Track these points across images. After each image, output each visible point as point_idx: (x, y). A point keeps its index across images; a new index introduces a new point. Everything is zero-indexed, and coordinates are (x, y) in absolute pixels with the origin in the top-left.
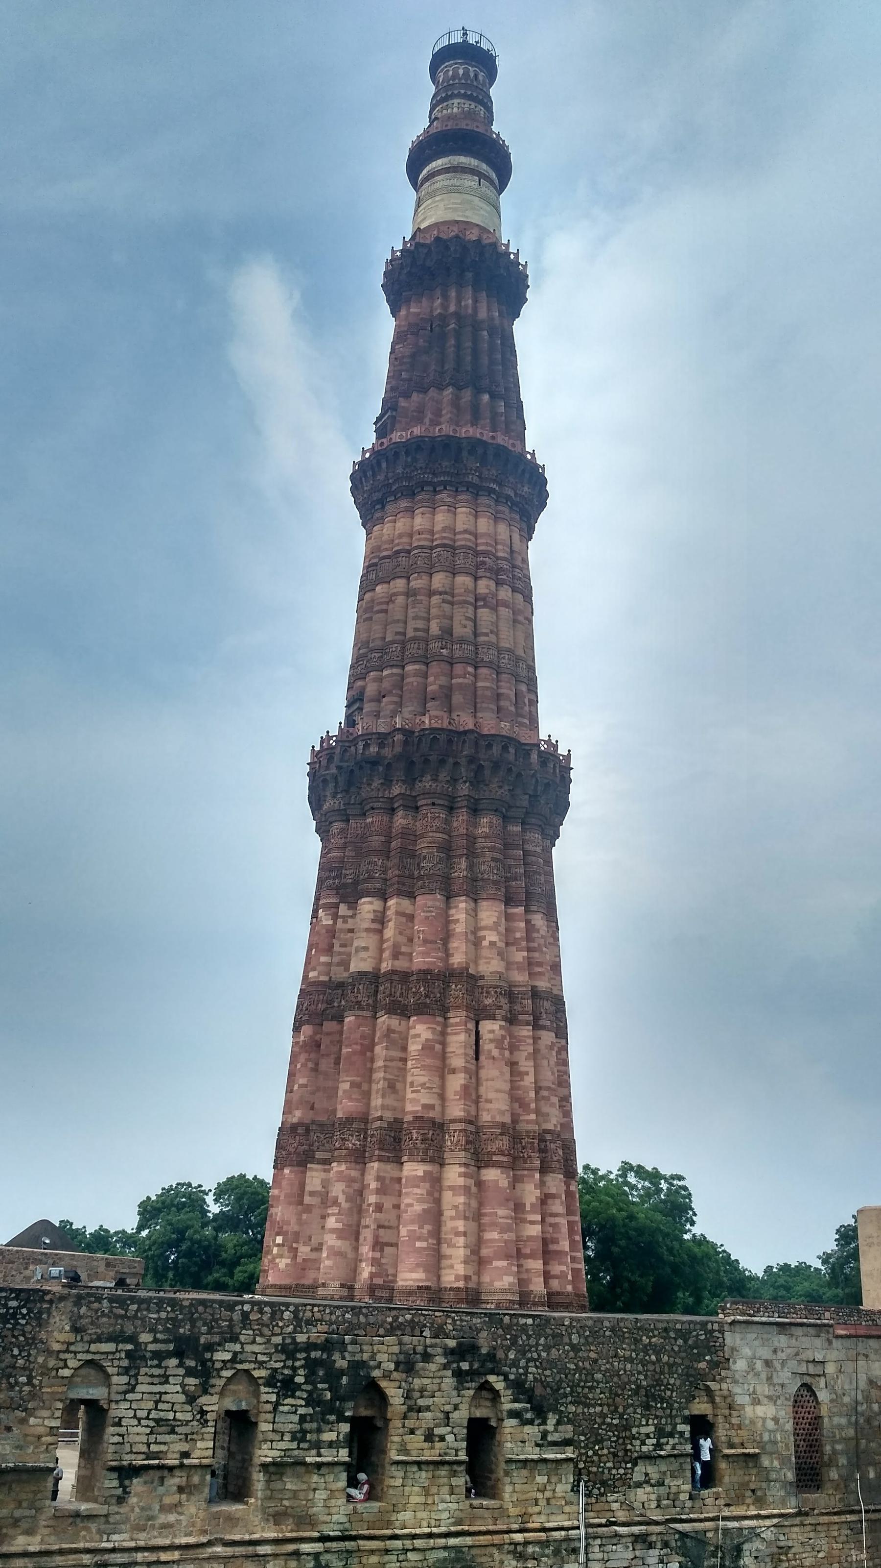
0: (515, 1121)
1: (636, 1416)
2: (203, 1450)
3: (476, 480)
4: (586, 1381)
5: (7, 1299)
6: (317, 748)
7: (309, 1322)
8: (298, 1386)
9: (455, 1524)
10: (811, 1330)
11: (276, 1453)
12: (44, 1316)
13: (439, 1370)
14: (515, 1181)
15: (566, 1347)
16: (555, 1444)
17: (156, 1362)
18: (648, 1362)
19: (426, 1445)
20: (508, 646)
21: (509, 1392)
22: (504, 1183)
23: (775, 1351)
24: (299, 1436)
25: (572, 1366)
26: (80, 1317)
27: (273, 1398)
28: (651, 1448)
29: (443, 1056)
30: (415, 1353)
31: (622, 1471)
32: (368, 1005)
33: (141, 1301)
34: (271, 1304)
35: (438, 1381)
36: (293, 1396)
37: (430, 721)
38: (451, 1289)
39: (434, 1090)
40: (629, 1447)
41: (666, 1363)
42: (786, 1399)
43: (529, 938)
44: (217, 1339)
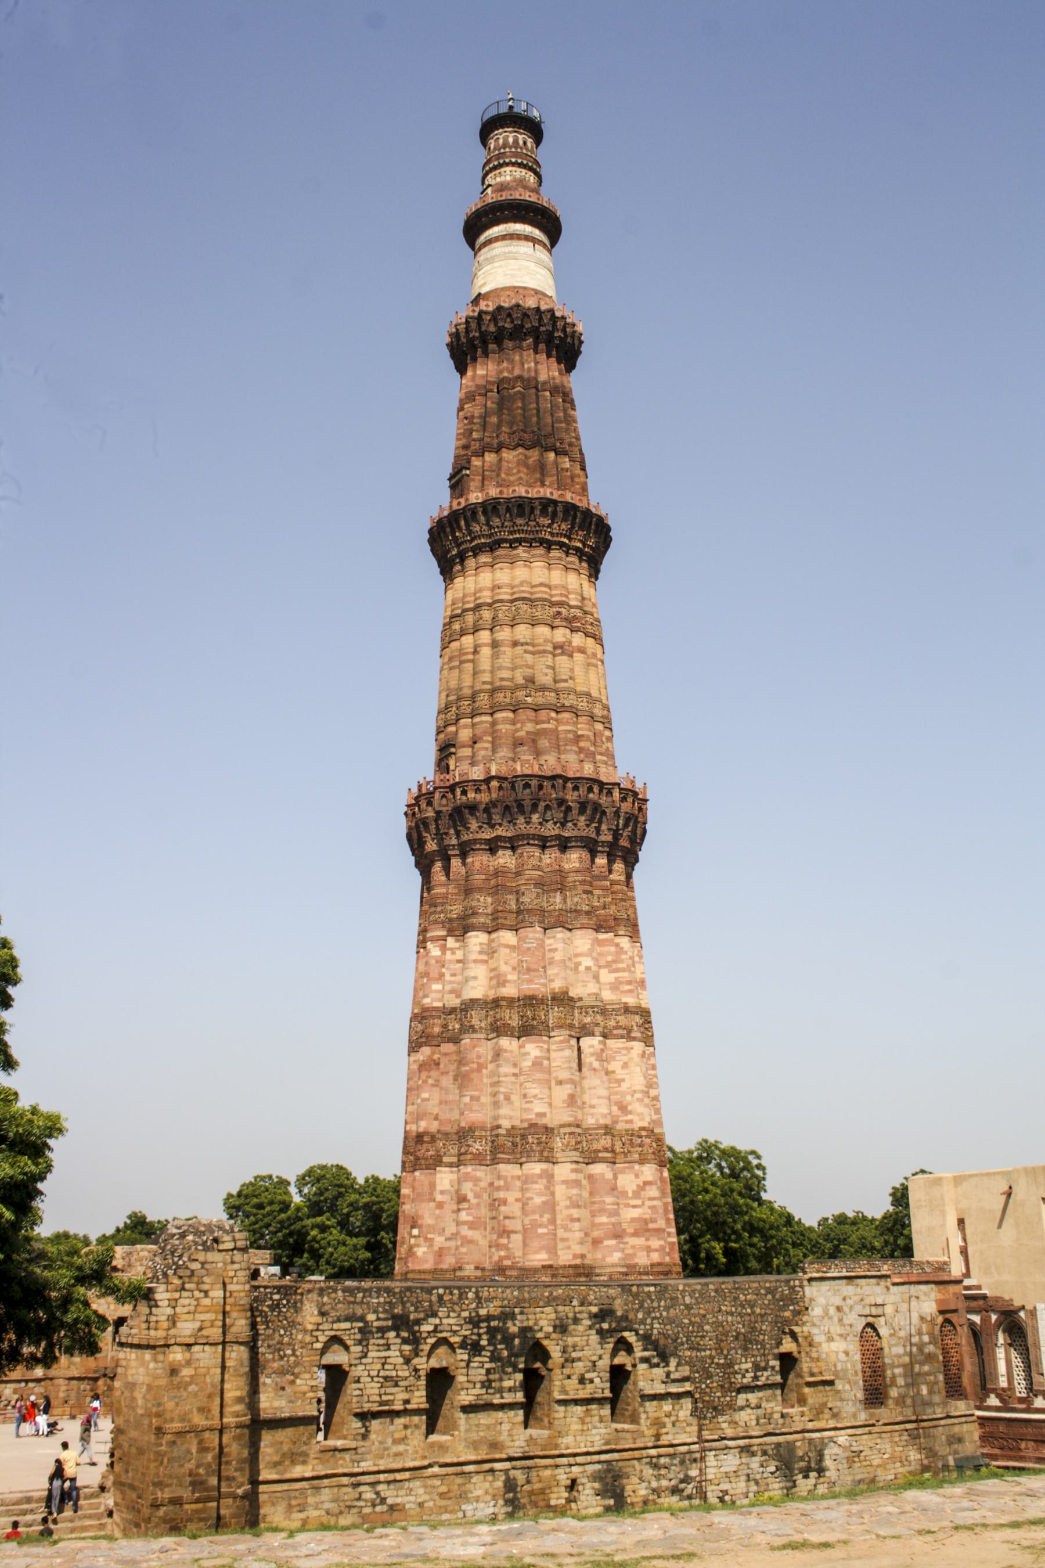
2: (419, 1398)
5: (272, 1293)
6: (415, 791)
8: (483, 1348)
10: (873, 1281)
11: (471, 1398)
12: (299, 1305)
16: (674, 1381)
17: (380, 1335)
19: (581, 1386)
21: (640, 1343)
22: (609, 1175)
23: (844, 1299)
24: (487, 1384)
25: (686, 1321)
26: (324, 1304)
27: (466, 1357)
30: (567, 1318)
31: (728, 1399)
33: (365, 1291)
34: (459, 1288)
36: (480, 1355)
37: (522, 766)
38: (570, 1266)
40: (733, 1380)
44: (422, 1315)
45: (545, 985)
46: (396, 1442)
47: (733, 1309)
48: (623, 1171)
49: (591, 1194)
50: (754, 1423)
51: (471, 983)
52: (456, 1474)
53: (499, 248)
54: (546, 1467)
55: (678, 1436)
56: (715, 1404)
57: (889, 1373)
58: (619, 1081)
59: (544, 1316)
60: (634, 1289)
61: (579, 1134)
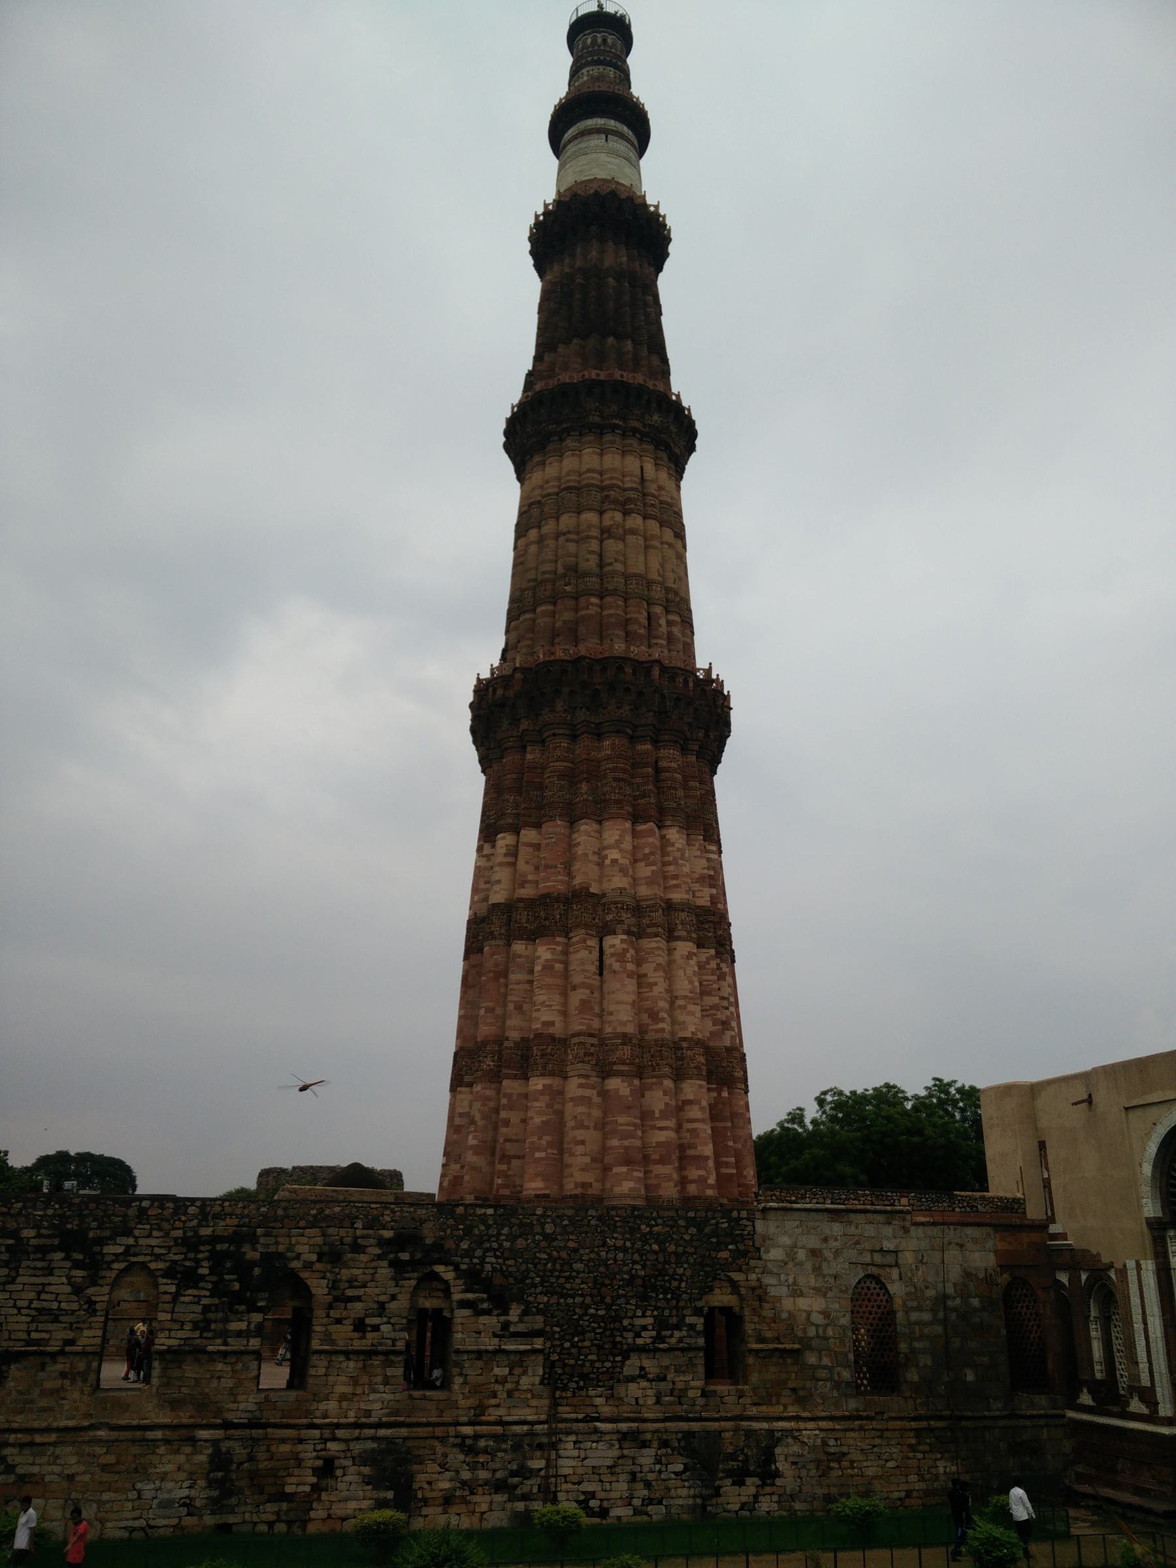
0: (642, 1029)
1: (628, 1307)
3: (597, 419)
4: (561, 1271)
7: (216, 1216)
8: (202, 1278)
9: (387, 1415)
10: (880, 1218)
14: (641, 1093)
15: (537, 1237)
17: (39, 1256)
18: (648, 1252)
19: (356, 1335)
21: (461, 1282)
23: (825, 1240)
27: (173, 1289)
29: (566, 975)
30: (342, 1244)
35: (372, 1271)
36: (196, 1287)
40: (618, 1339)
42: (841, 1291)
43: (664, 853)
44: (107, 1233)
45: (561, 882)
46: (44, 1393)
49: (605, 1113)
50: (651, 1401)
51: (496, 888)
52: (133, 1441)
54: (283, 1441)
55: (513, 1411)
57: (903, 1346)
58: (651, 985)
59: (305, 1240)
60: (460, 1210)
61: (592, 1045)
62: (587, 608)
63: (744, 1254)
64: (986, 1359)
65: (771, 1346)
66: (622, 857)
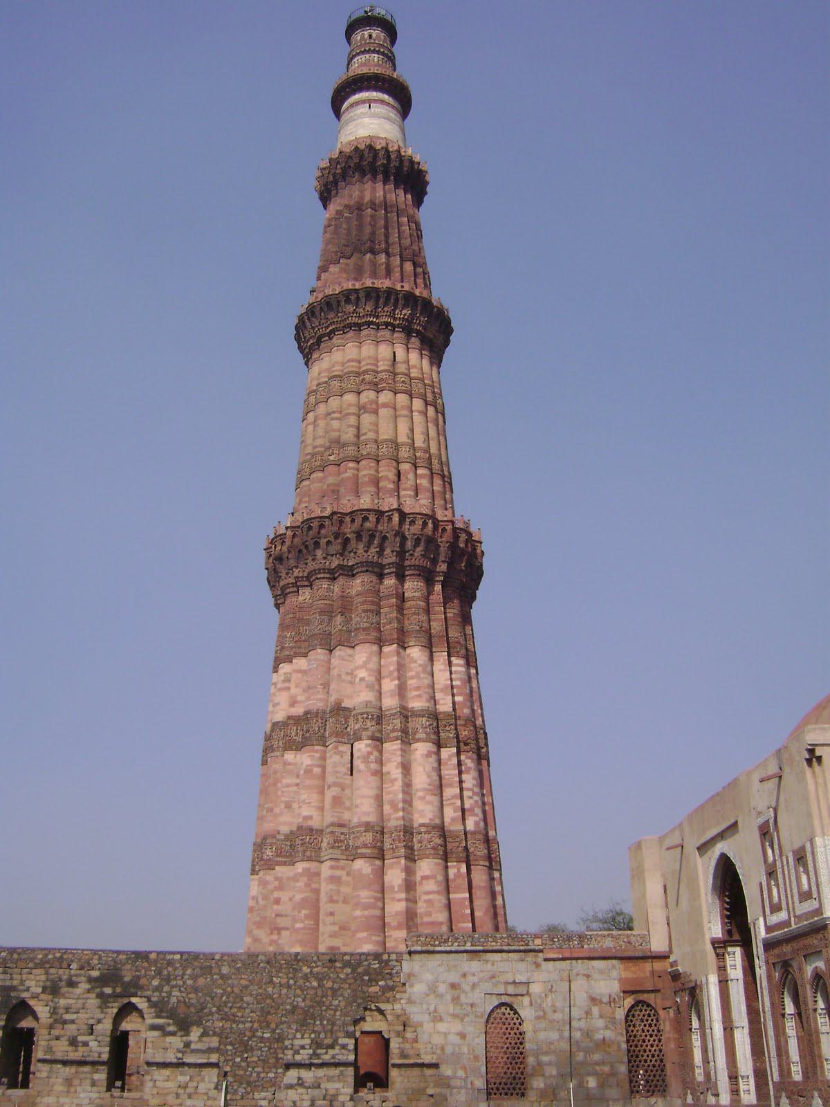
3: (355, 320)
4: (235, 1002)
13: (84, 994)
15: (215, 977)
18: (308, 988)
19: (70, 1048)
20: (386, 437)
21: (153, 1010)
23: (464, 975)
25: (219, 991)
28: (306, 1057)
29: (323, 776)
30: (61, 980)
32: (278, 747)
35: (81, 1001)
39: (313, 804)
40: (281, 1056)
41: (330, 988)
42: (477, 1016)
45: (321, 700)
47: (291, 982)
48: (391, 867)
53: (344, 118)
56: (252, 1079)
57: (531, 1060)
59: (32, 977)
61: (342, 834)
62: (346, 472)
63: (392, 989)
64: (606, 1069)
65: (412, 1061)
66: (369, 675)
